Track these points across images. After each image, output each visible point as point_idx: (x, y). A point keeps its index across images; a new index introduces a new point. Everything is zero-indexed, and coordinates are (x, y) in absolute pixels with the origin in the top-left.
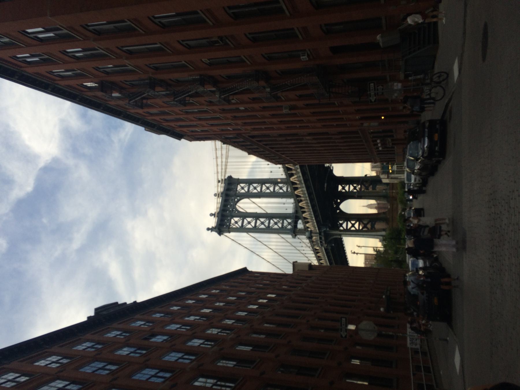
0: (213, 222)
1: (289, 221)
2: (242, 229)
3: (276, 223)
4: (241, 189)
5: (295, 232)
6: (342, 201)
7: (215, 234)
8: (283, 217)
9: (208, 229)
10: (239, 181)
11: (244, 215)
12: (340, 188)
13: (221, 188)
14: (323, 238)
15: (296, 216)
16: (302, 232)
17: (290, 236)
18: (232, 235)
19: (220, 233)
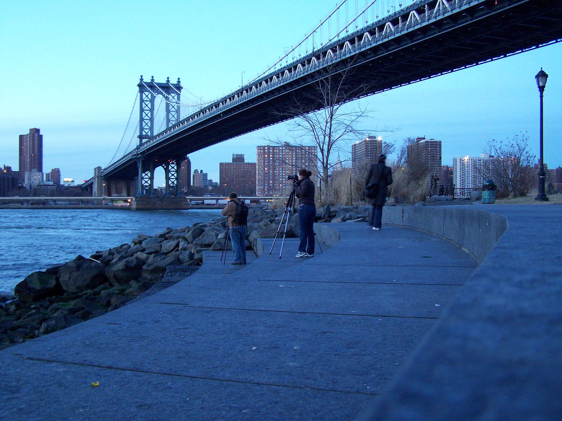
0: (147, 79)
1: (149, 134)
2: (142, 101)
3: (147, 124)
4: (173, 97)
5: (141, 137)
6: (163, 167)
7: (138, 82)
8: (151, 129)
9: (142, 76)
10: (179, 95)
11: (152, 101)
12: (173, 165)
13: (173, 81)
14: (135, 157)
15: (152, 138)
16: (141, 141)
17: (138, 134)
18: (139, 93)
19: (138, 85)
